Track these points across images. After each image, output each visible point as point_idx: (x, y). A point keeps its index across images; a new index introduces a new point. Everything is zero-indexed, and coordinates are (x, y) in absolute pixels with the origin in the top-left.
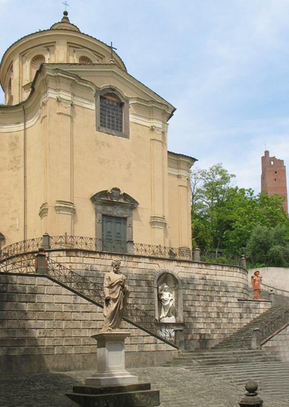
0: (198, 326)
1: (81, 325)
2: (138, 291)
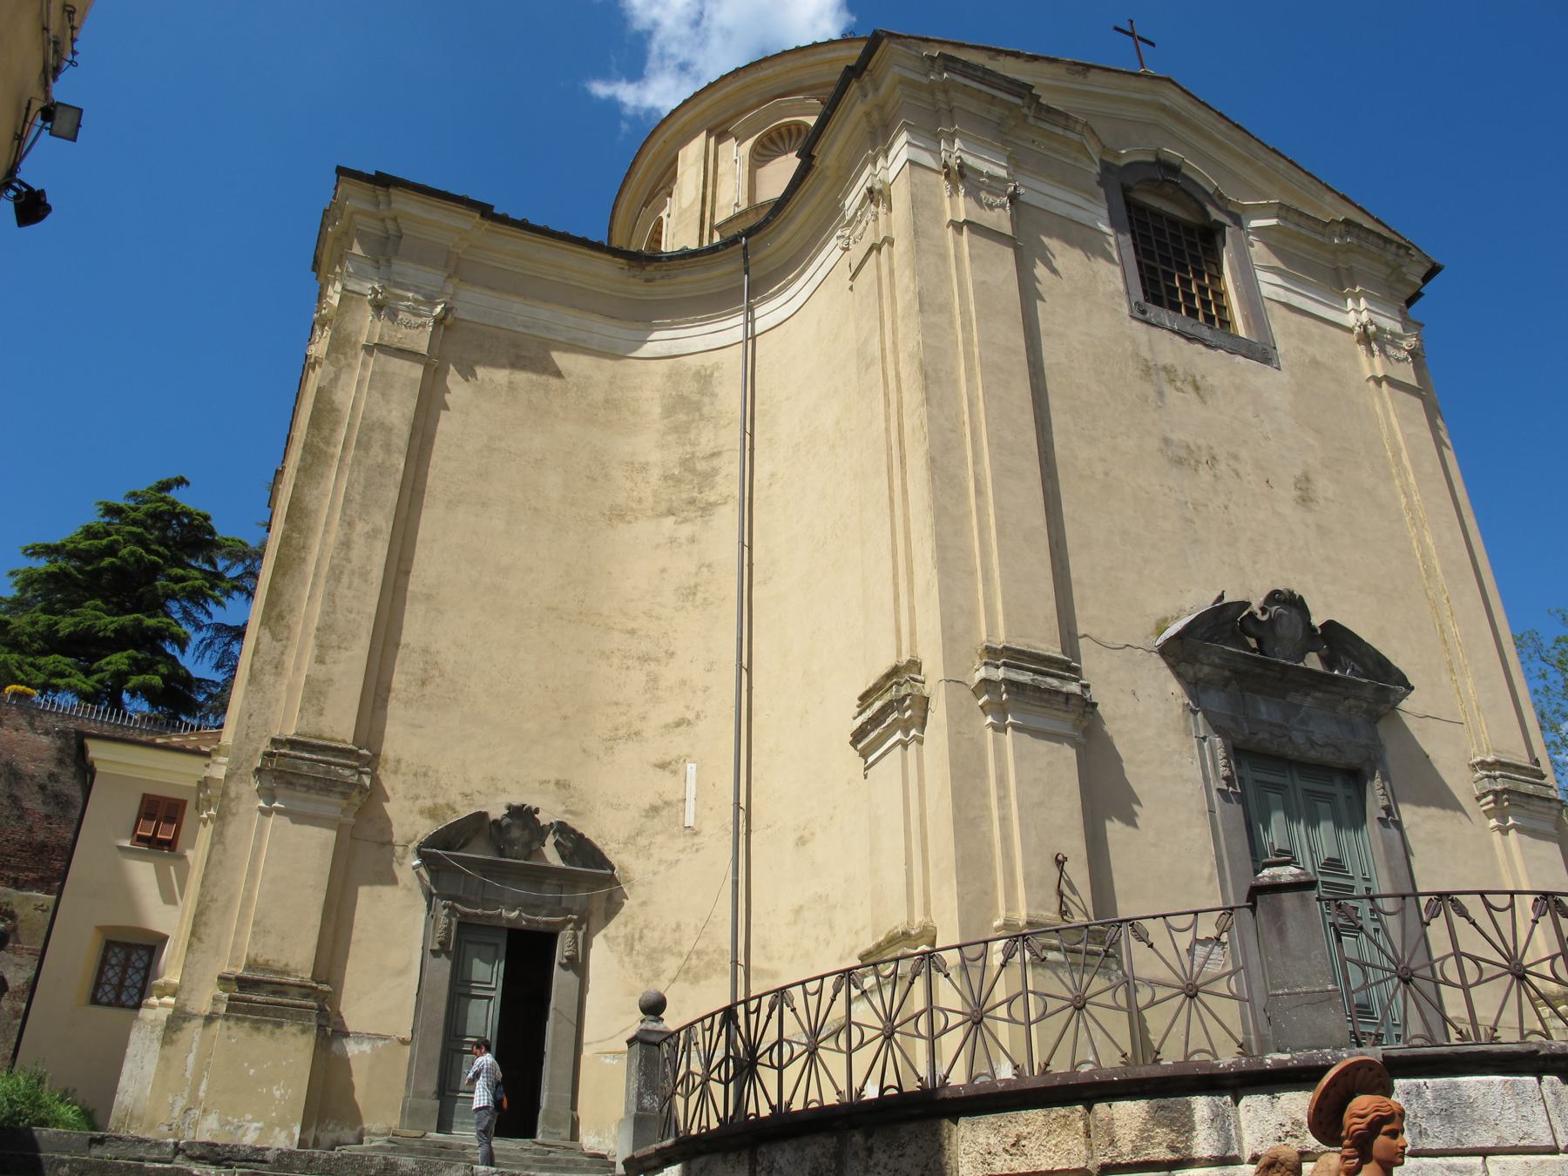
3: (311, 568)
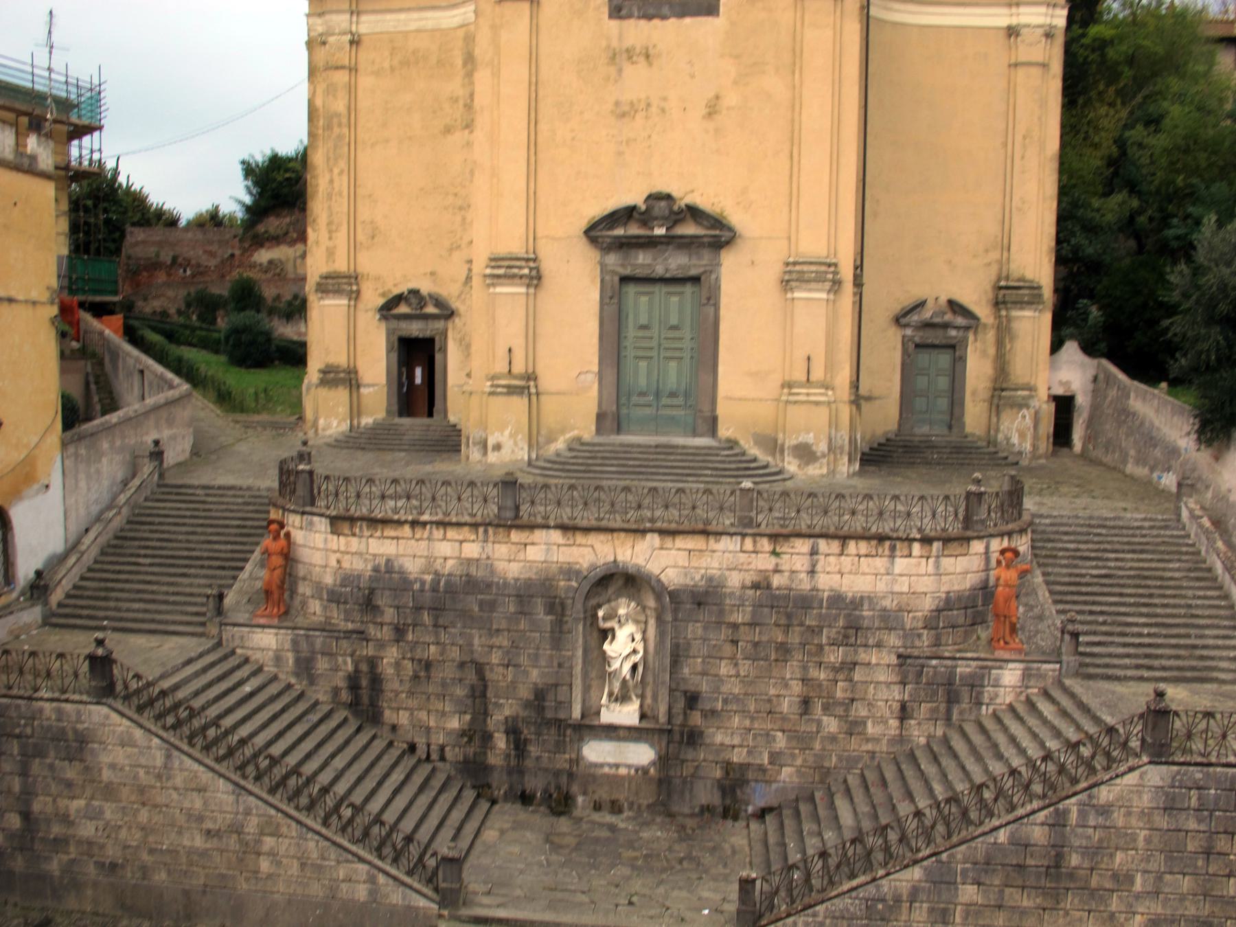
0: (719, 738)
1: (181, 819)
2: (522, 627)
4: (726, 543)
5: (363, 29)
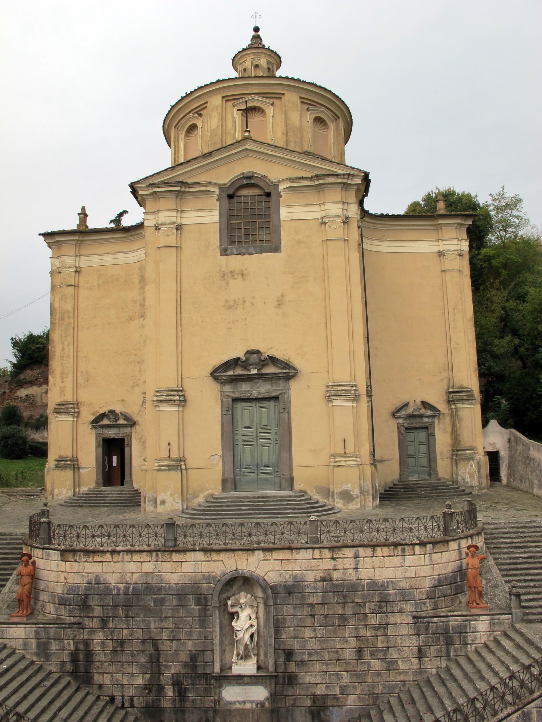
0: (307, 679)
2: (181, 615)
3: (57, 357)
4: (303, 554)
5: (82, 265)
